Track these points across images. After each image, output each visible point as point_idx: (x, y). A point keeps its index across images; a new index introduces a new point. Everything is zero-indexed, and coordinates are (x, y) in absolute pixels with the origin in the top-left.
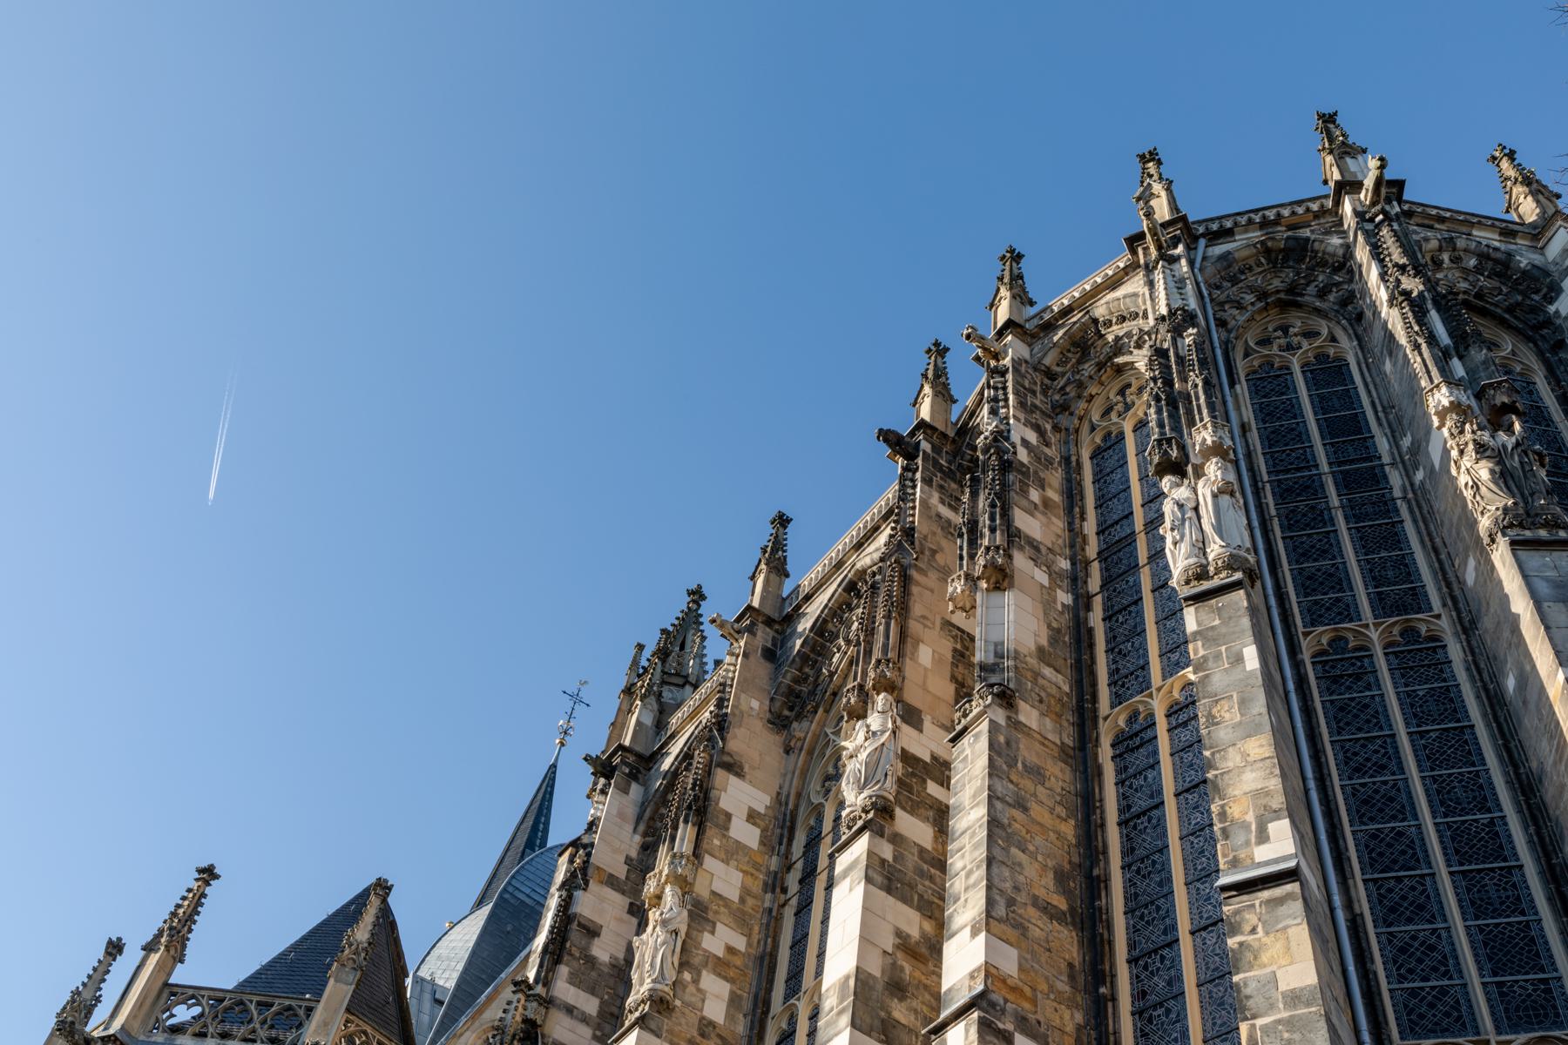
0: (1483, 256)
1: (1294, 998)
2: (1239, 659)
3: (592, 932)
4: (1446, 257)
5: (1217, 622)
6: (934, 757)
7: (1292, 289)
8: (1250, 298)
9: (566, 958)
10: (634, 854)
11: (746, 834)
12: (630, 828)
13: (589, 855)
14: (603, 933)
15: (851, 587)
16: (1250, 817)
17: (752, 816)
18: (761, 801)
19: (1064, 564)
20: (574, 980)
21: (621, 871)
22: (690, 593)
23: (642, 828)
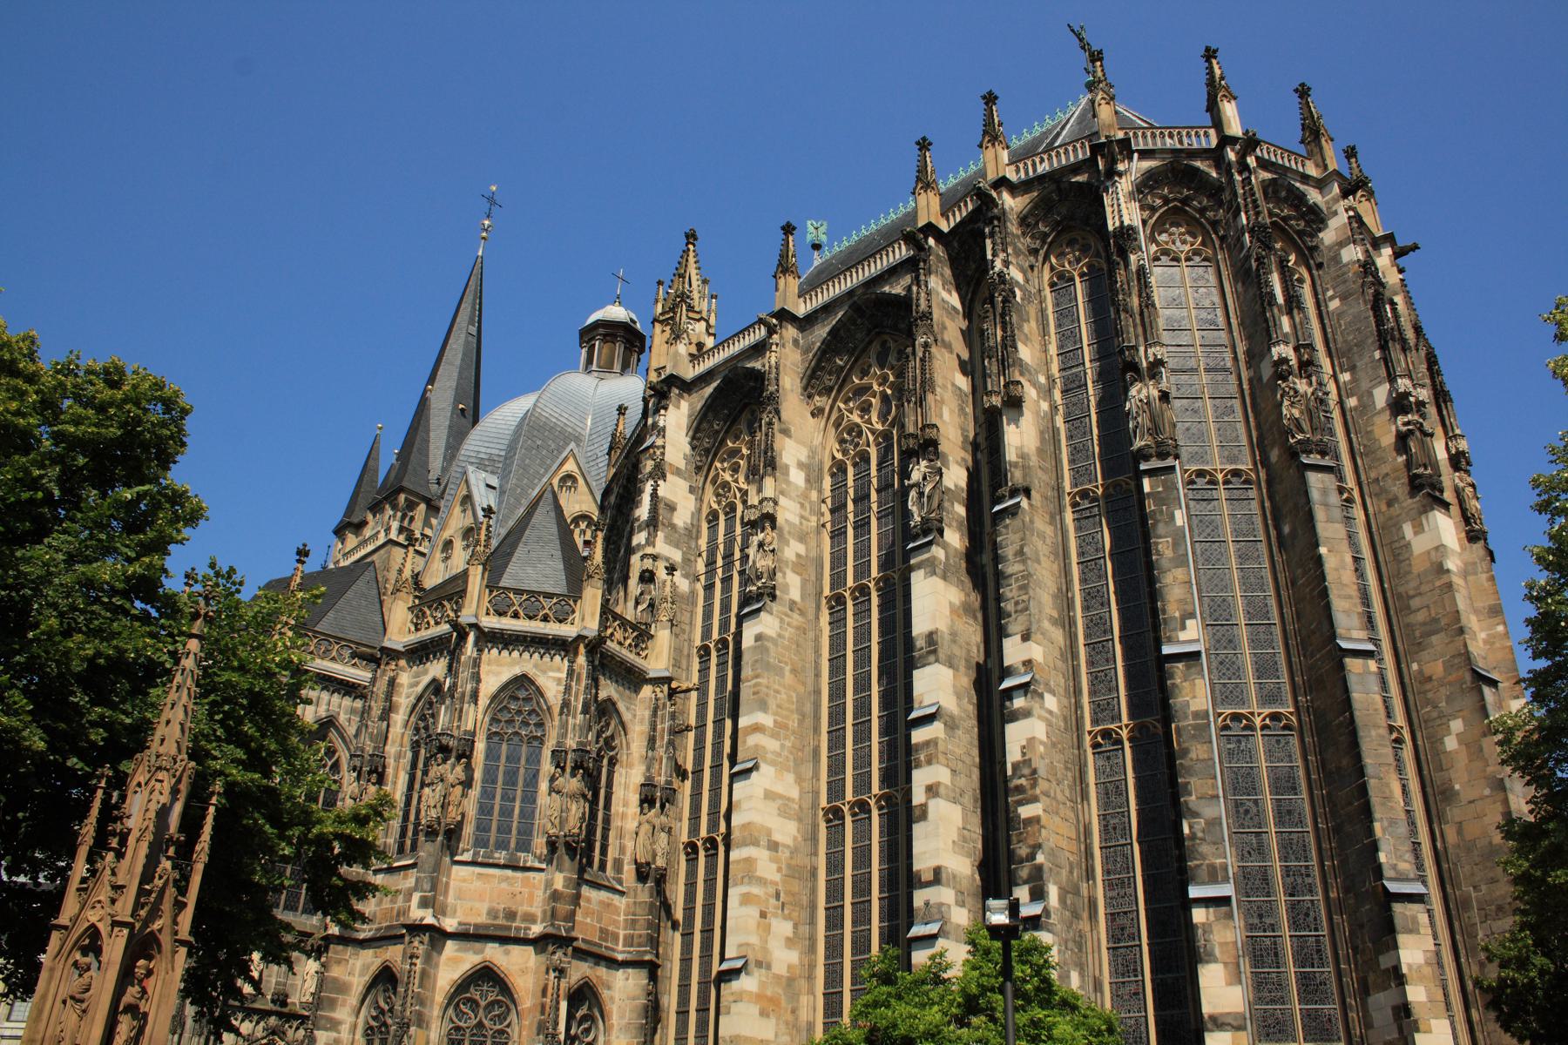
0: (1292, 190)
1: (1196, 715)
2: (1172, 517)
3: (672, 508)
4: (1270, 190)
5: (1160, 489)
6: (956, 486)
7: (1186, 201)
8: (1158, 202)
9: (660, 527)
10: (688, 449)
11: (797, 477)
12: (684, 433)
13: (663, 454)
14: (678, 507)
15: (857, 309)
16: (1177, 614)
17: (801, 465)
18: (803, 455)
19: (1042, 379)
20: (668, 540)
21: (682, 464)
22: (687, 236)
23: (691, 433)
